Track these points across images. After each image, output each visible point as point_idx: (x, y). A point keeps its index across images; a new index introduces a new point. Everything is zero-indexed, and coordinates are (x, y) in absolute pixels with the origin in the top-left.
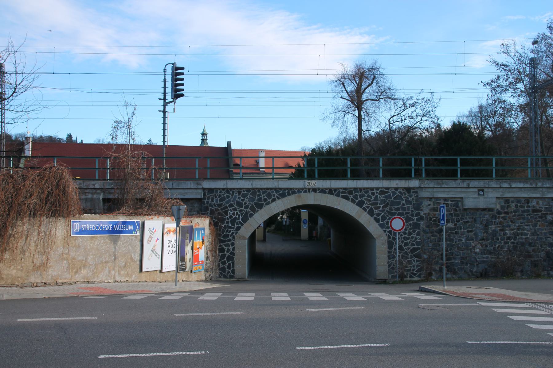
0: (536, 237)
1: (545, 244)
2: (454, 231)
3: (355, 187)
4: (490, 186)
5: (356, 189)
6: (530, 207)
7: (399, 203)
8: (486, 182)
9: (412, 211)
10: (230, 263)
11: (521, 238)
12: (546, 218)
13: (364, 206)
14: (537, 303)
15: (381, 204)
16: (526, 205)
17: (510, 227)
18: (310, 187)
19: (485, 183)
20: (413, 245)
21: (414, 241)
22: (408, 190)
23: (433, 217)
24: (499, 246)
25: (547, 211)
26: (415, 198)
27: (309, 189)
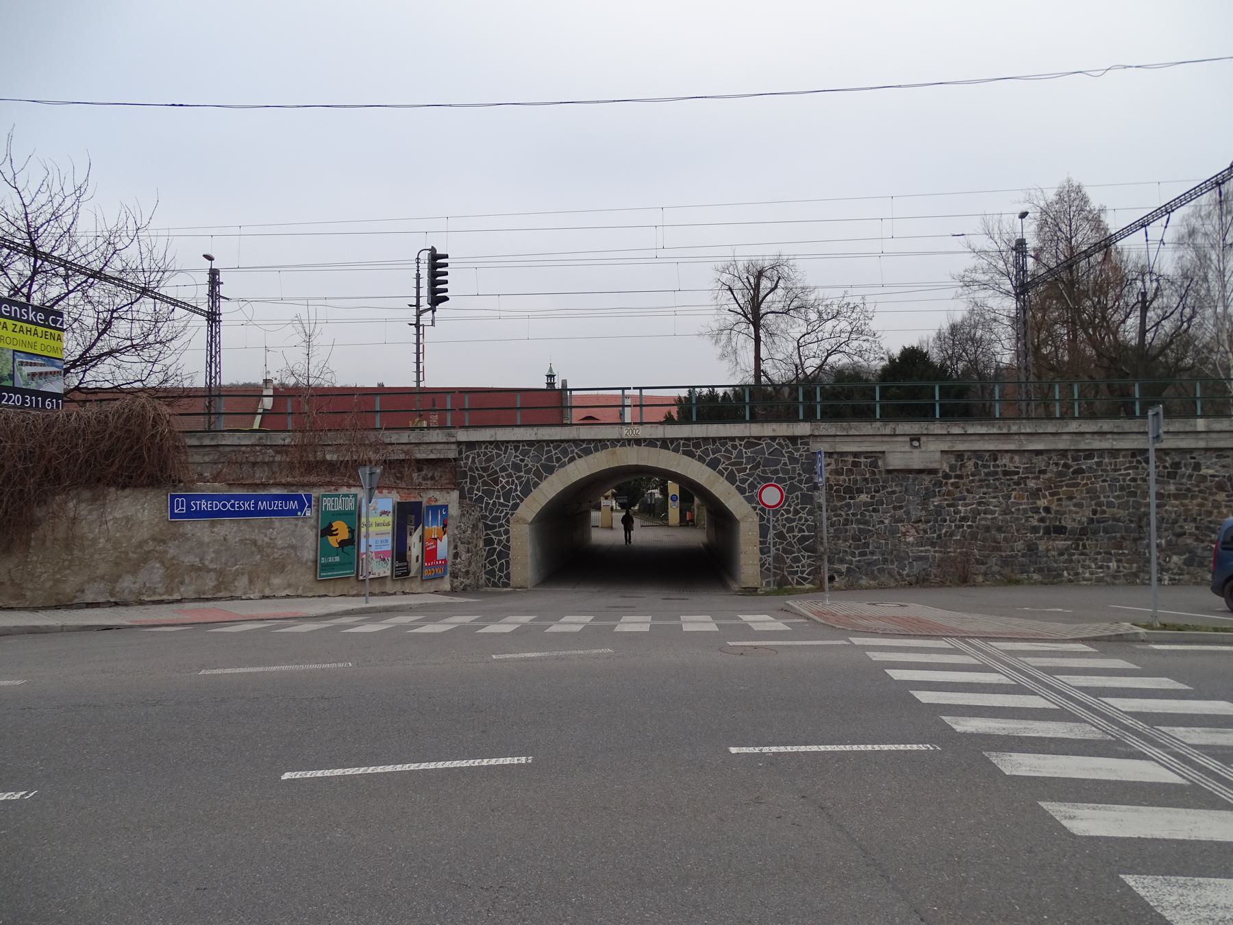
0: (1008, 517)
1: (1024, 529)
2: (871, 508)
3: (705, 436)
4: (930, 433)
5: (706, 439)
6: (998, 466)
7: (777, 462)
8: (924, 425)
9: (799, 475)
10: (503, 563)
11: (985, 519)
12: (1026, 485)
13: (720, 467)
14: (969, 637)
15: (748, 463)
16: (993, 463)
17: (965, 499)
18: (630, 437)
19: (922, 428)
20: (801, 530)
21: (803, 525)
22: (793, 439)
23: (835, 485)
24: (947, 532)
25: (1027, 473)
26: (804, 453)
27: (629, 441)
